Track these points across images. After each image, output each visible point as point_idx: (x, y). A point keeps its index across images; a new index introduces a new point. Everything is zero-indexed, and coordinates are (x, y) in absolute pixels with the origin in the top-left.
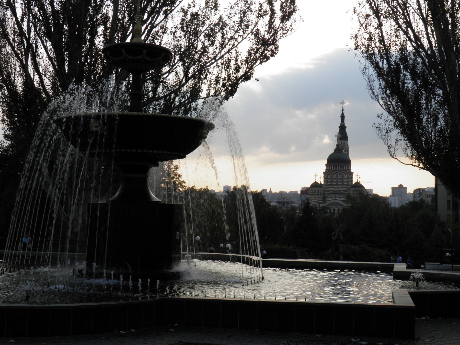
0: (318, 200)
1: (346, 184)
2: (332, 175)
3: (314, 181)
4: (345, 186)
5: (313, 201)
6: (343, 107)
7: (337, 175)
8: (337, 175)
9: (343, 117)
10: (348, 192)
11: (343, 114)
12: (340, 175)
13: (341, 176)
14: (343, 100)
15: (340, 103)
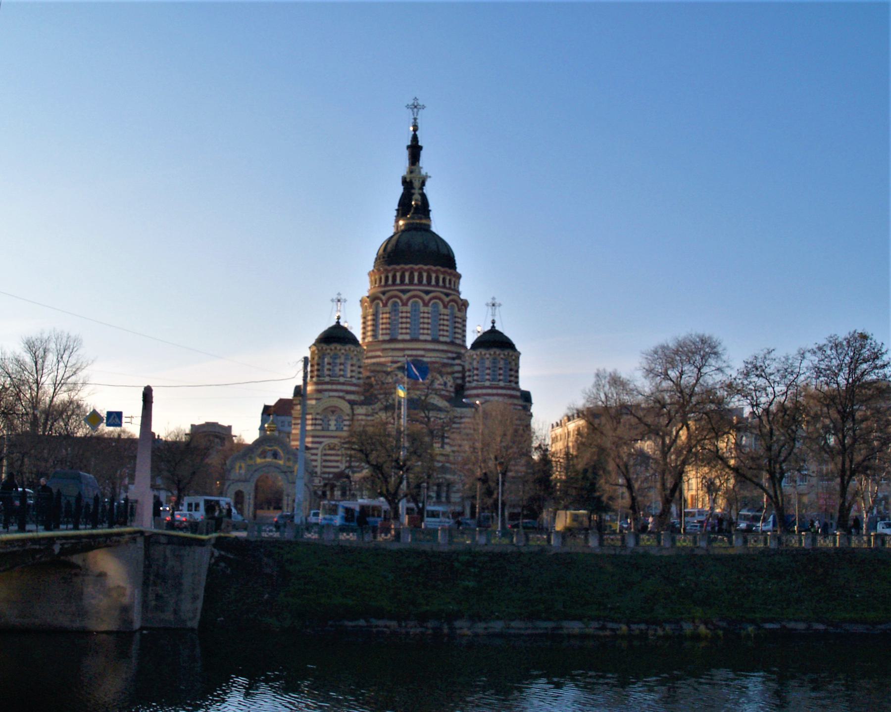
0: (348, 392)
1: (448, 340)
2: (395, 304)
3: (333, 323)
4: (445, 347)
5: (327, 394)
6: (415, 119)
7: (415, 304)
8: (415, 304)
9: (415, 150)
10: (459, 368)
11: (415, 138)
12: (426, 304)
13: (428, 309)
14: (416, 99)
15: (408, 107)
